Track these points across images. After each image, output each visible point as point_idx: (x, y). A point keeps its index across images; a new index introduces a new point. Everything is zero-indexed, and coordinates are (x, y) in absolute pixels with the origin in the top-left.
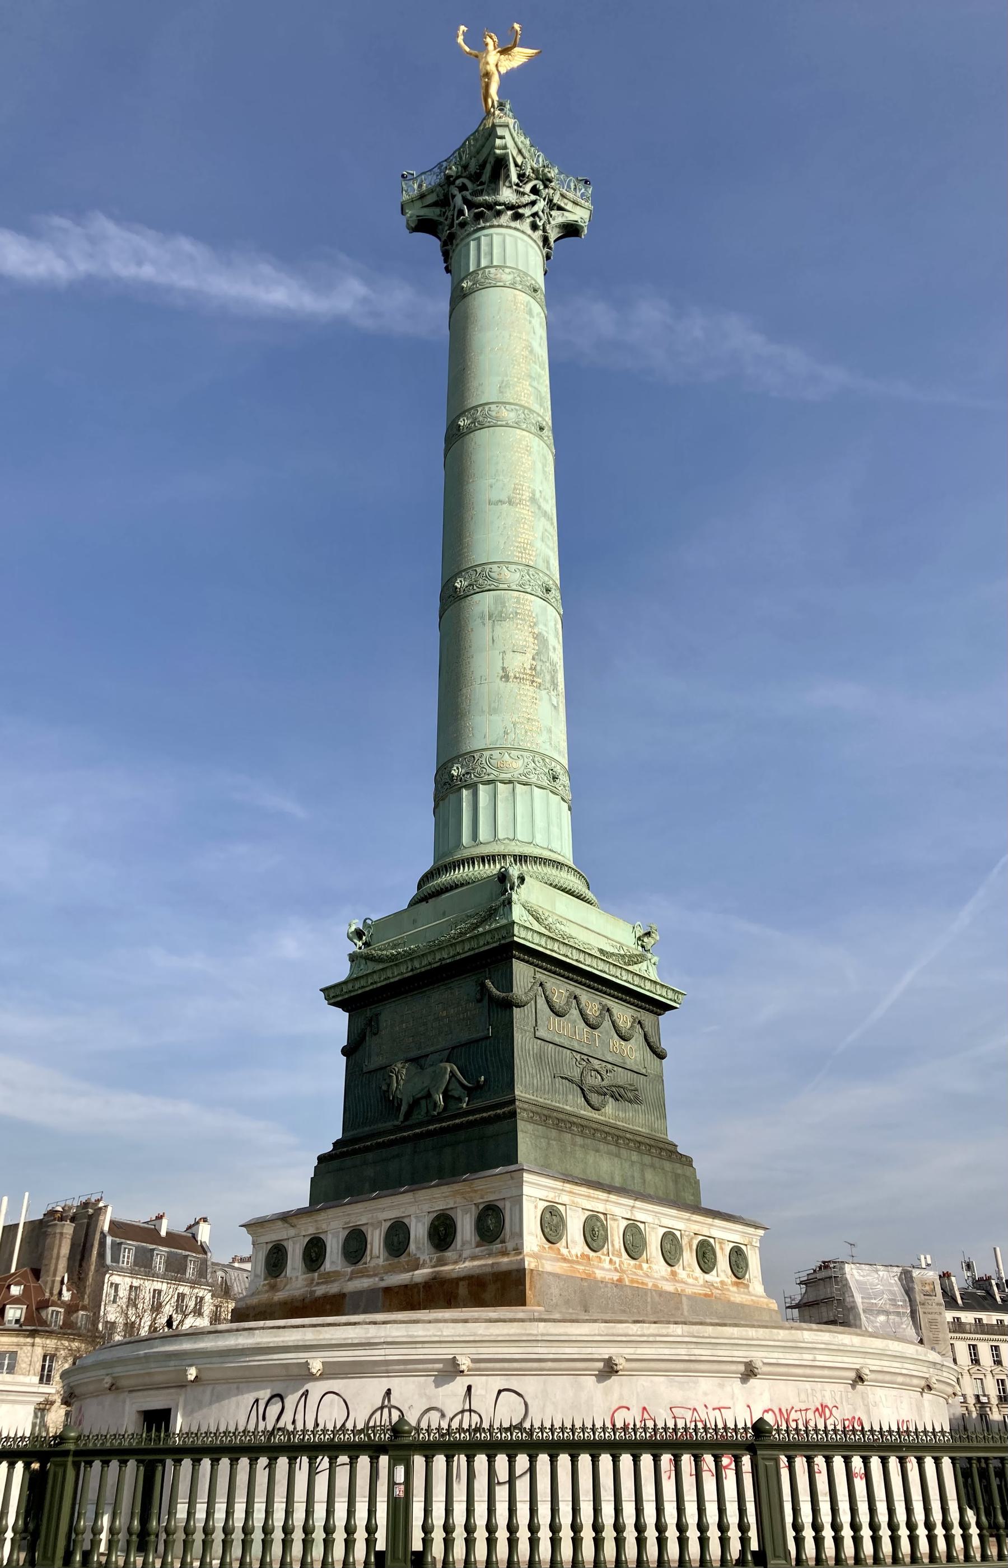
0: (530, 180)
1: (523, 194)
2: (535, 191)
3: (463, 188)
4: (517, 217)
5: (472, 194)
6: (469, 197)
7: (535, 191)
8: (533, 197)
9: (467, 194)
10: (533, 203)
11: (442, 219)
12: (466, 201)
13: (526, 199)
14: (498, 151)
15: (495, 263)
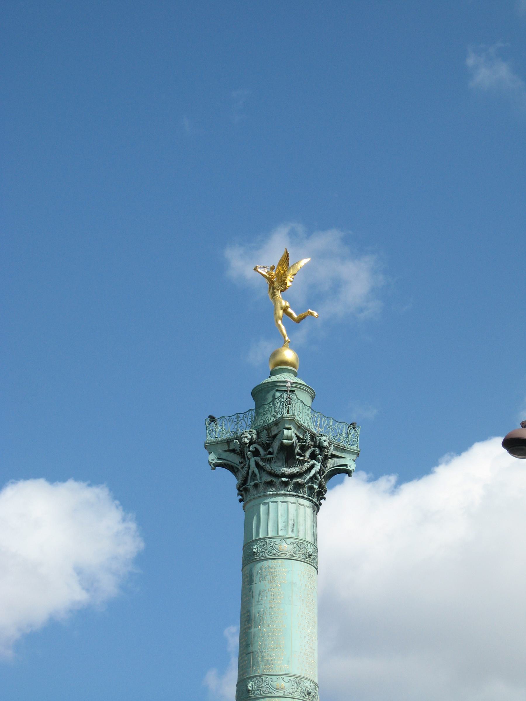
0: (309, 447)
1: (304, 462)
2: (313, 456)
3: (256, 453)
4: (298, 487)
5: (262, 459)
6: (261, 463)
7: (313, 456)
8: (312, 462)
9: (258, 459)
10: (313, 466)
11: (239, 468)
12: (257, 465)
13: (307, 466)
14: (284, 441)
15: (281, 534)
